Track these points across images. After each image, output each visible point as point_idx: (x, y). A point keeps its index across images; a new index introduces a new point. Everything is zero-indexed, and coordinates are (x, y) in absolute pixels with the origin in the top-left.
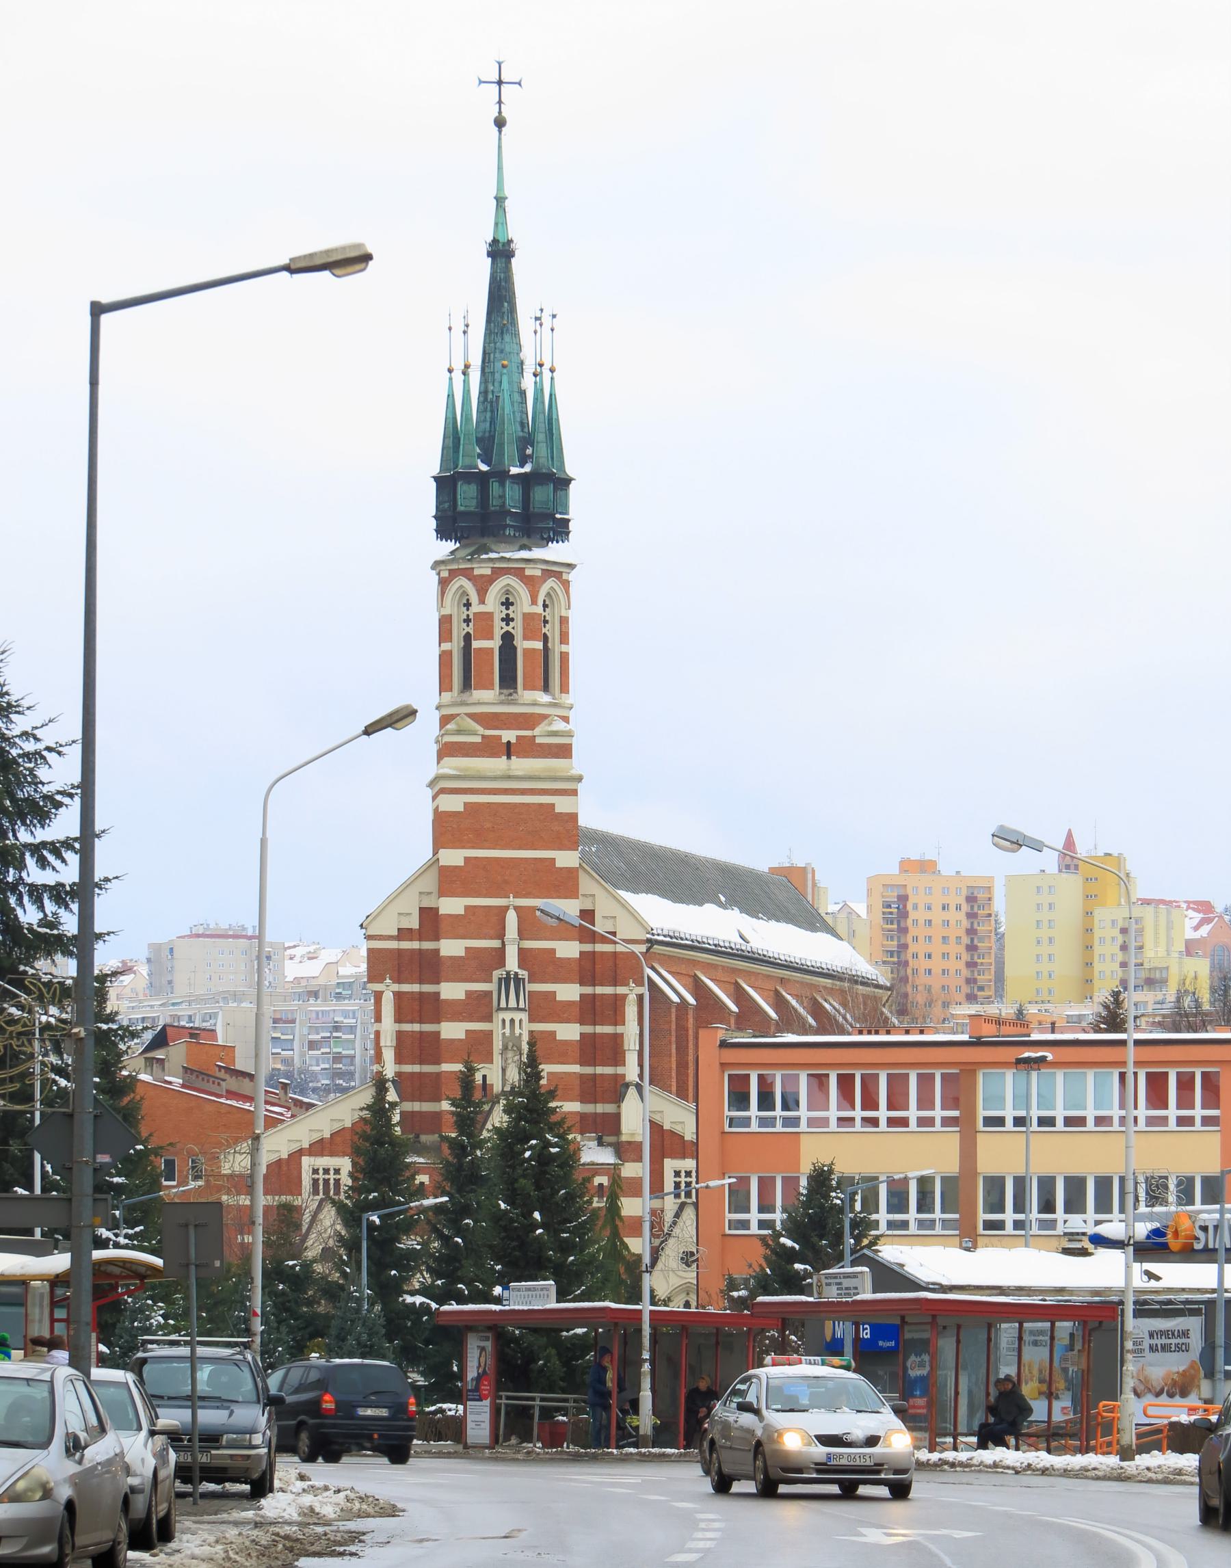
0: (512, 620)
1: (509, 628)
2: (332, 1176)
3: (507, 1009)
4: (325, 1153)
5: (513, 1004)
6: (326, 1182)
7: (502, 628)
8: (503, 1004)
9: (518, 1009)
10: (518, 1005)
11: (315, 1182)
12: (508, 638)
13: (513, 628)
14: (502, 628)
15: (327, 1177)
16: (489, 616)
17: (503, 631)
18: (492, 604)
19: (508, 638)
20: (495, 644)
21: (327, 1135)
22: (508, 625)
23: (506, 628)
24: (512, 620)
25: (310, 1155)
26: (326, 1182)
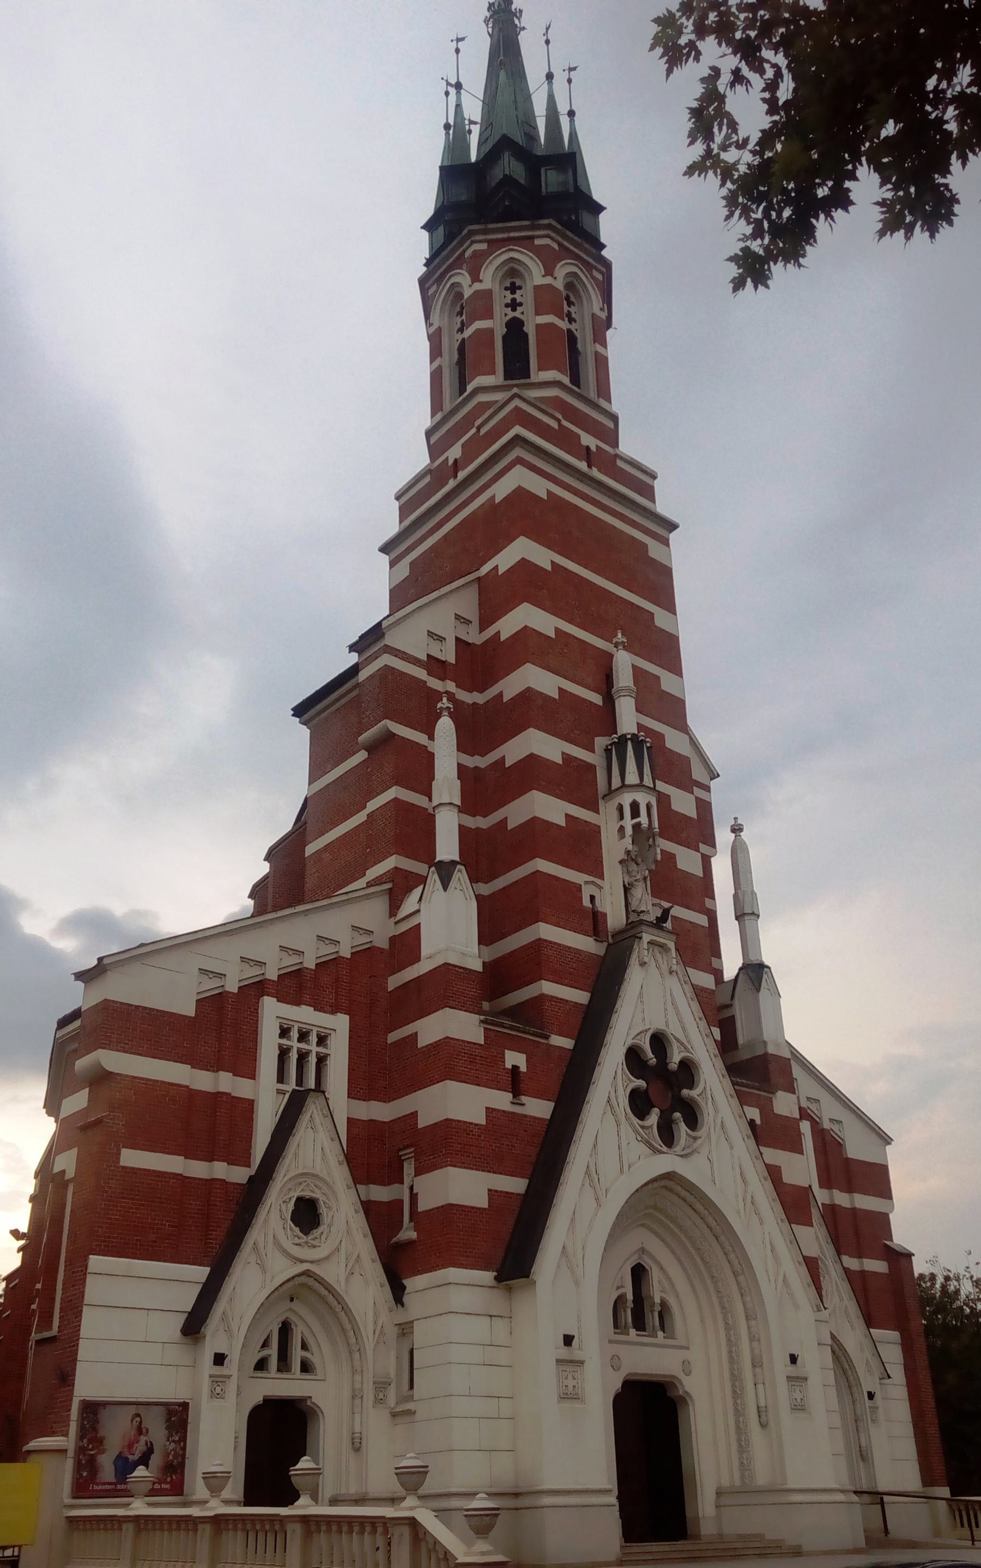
0: (521, 304)
1: (517, 314)
2: (312, 1046)
3: (624, 786)
4: (307, 997)
5: (632, 777)
6: (303, 1056)
7: (506, 315)
8: (616, 782)
9: (641, 786)
10: (642, 779)
11: (283, 1053)
12: (515, 327)
13: (523, 313)
14: (506, 315)
15: (303, 1046)
16: (488, 294)
17: (508, 318)
18: (489, 278)
19: (515, 327)
20: (497, 324)
21: (310, 963)
22: (514, 310)
23: (511, 314)
24: (521, 304)
25: (282, 998)
26: (303, 1057)
